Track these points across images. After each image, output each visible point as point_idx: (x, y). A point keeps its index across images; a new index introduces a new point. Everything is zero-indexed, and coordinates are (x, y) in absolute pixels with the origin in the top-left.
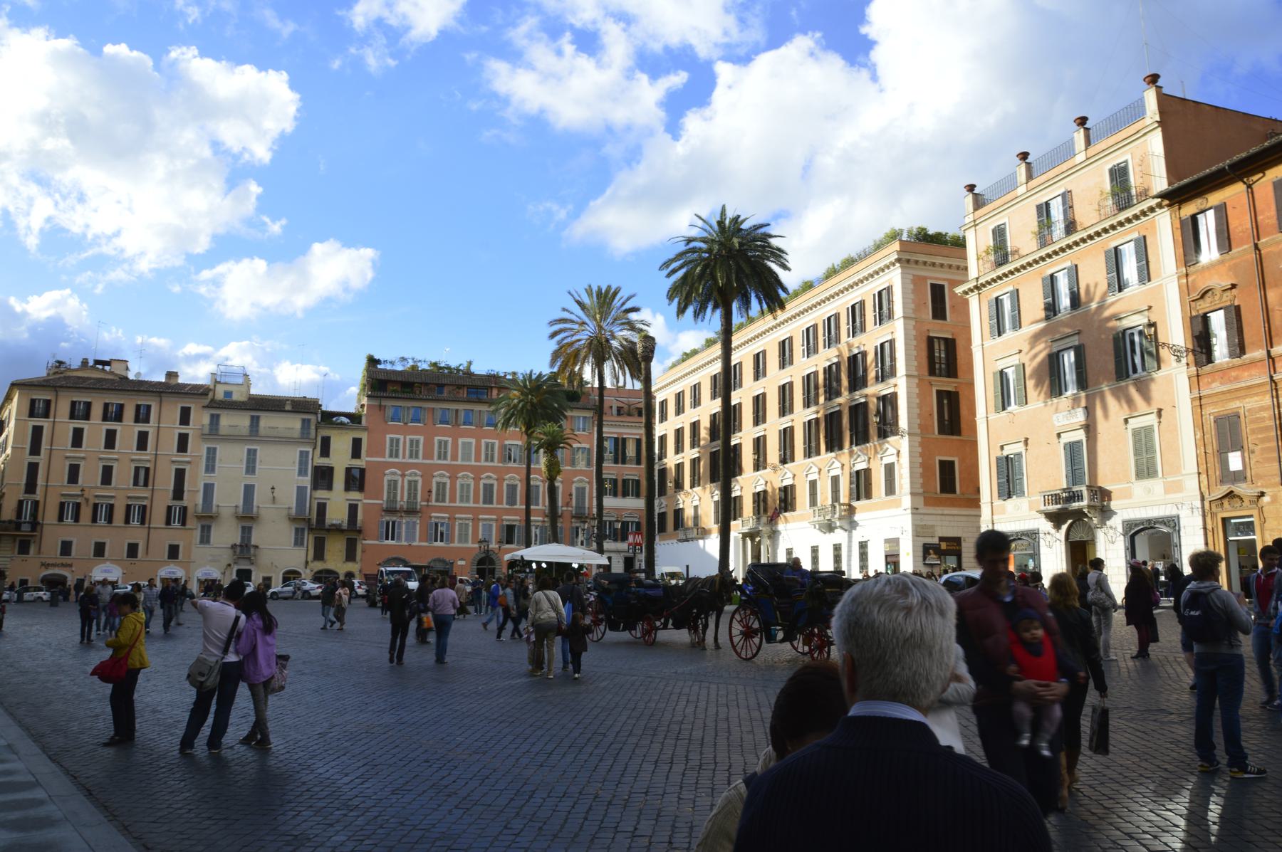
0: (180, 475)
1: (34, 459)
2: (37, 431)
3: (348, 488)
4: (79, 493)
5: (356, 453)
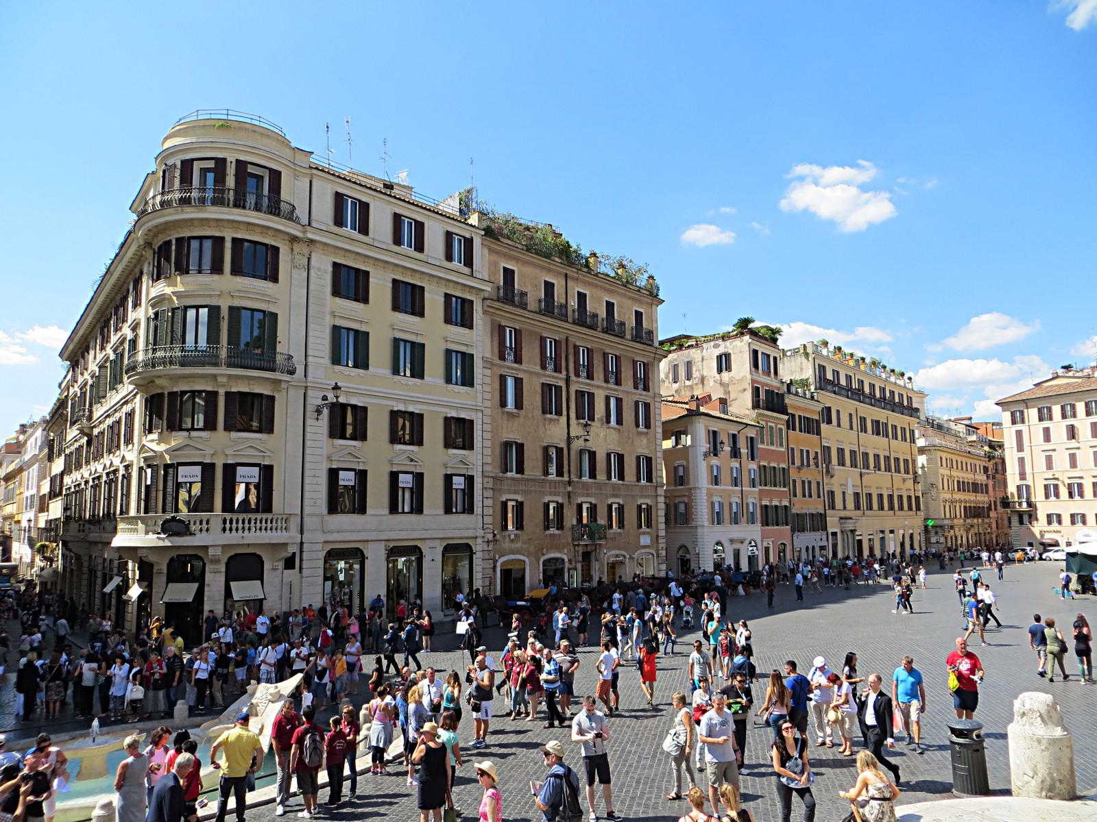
1: (1021, 455)
2: (1019, 434)
4: (1052, 477)
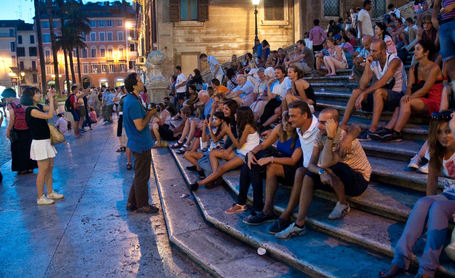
3: (31, 55)
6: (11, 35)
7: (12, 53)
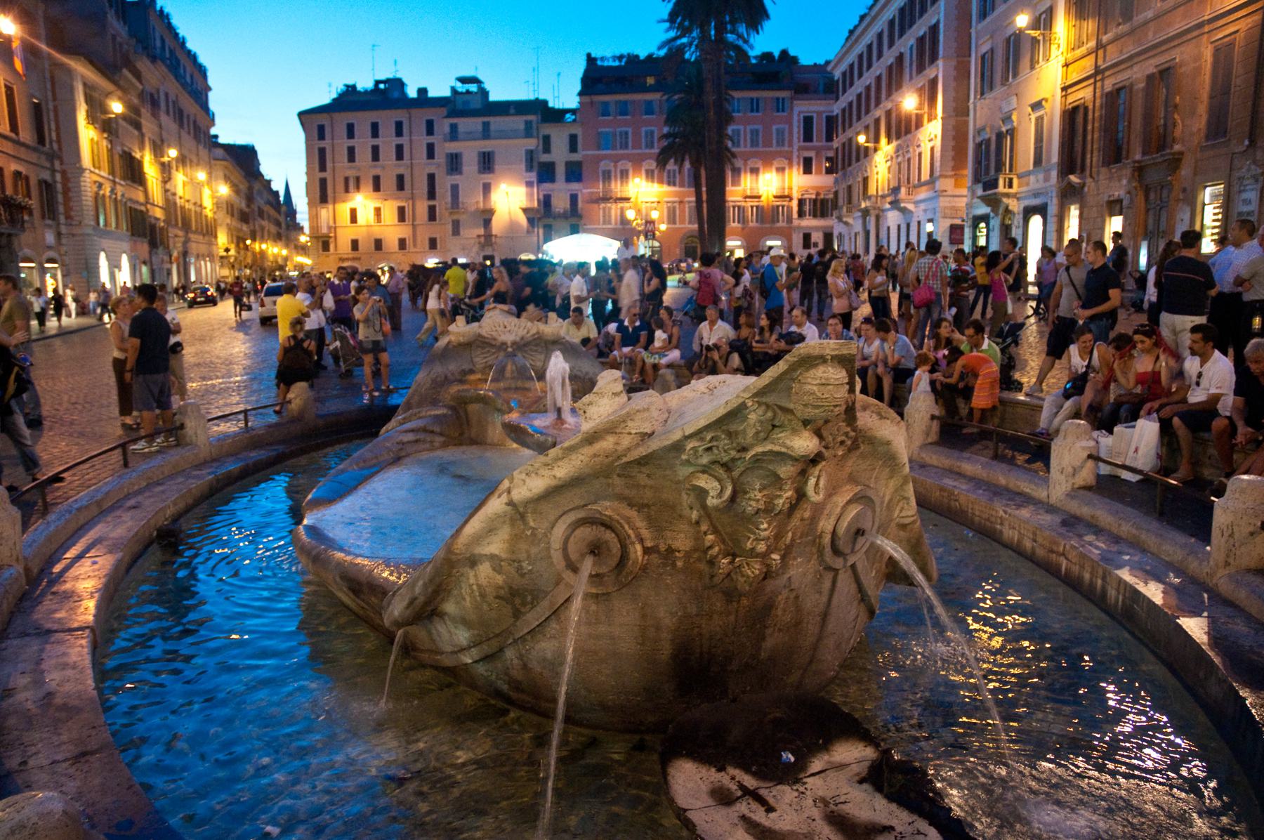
0: (431, 178)
1: (323, 175)
5: (573, 147)
6: (528, 133)
7: (528, 174)
